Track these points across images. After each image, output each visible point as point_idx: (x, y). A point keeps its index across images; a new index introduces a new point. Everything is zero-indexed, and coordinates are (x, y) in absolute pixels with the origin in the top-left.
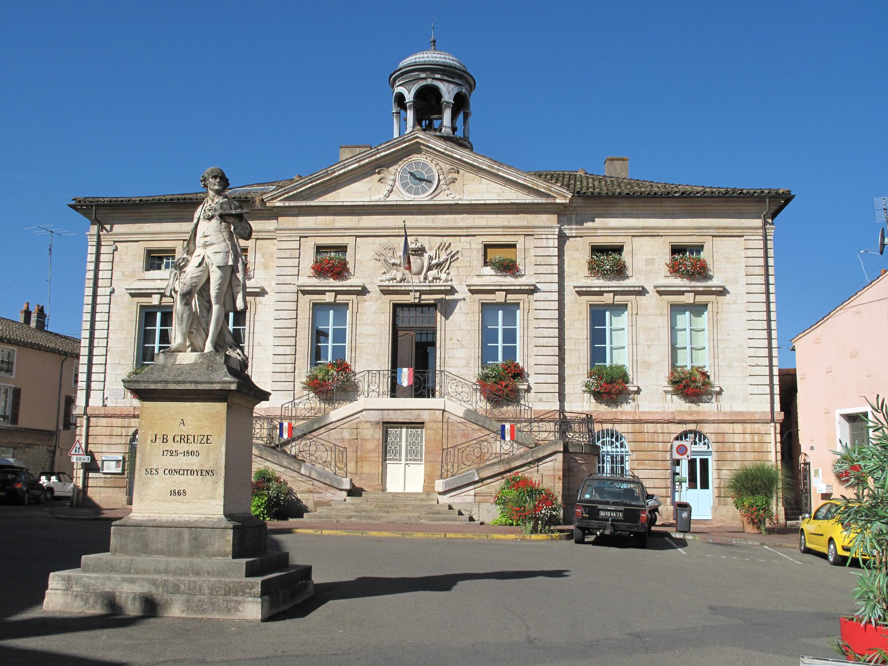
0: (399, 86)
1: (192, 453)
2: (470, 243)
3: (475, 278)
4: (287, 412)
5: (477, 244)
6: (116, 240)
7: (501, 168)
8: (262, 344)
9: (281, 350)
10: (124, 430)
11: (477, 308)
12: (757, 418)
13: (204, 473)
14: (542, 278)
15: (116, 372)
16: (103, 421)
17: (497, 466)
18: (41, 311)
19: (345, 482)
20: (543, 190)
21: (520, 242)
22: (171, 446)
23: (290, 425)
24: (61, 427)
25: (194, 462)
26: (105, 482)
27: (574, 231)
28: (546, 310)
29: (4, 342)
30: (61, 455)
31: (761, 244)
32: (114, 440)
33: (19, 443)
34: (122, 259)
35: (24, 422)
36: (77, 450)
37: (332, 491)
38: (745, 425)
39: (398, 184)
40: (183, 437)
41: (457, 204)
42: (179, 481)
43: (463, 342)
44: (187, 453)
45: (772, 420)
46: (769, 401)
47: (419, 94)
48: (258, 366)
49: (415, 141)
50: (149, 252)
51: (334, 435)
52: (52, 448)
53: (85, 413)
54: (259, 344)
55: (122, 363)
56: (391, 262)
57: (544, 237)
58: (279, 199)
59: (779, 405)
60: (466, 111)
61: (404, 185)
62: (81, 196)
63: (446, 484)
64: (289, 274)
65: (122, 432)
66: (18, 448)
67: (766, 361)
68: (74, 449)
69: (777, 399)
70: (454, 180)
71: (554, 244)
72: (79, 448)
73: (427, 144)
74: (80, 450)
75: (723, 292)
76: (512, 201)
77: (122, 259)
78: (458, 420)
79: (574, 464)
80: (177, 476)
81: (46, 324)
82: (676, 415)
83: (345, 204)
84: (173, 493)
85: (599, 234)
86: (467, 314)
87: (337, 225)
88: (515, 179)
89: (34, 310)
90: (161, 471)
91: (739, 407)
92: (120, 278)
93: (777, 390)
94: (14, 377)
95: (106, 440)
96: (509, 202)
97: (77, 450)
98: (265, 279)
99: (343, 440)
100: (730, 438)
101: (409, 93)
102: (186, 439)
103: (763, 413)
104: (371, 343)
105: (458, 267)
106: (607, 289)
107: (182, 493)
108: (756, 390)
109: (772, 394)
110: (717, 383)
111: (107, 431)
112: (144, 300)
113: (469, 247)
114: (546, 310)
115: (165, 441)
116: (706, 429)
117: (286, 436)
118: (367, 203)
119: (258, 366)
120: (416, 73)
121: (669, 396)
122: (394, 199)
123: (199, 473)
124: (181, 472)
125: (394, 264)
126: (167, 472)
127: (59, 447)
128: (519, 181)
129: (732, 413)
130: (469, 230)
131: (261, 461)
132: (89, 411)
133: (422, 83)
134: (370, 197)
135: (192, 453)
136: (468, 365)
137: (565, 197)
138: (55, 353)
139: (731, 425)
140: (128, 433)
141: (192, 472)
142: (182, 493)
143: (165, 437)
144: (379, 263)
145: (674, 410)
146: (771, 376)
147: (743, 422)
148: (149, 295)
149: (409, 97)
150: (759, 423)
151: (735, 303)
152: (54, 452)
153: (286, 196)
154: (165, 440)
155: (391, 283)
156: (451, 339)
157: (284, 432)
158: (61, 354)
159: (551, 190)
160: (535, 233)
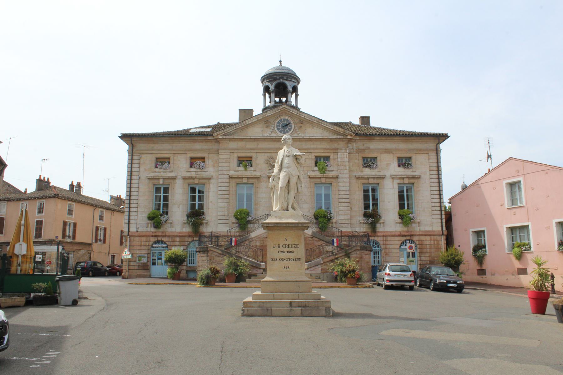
0: (266, 82)
1: (291, 252)
2: (309, 156)
3: (312, 172)
4: (230, 233)
5: (312, 156)
6: (141, 153)
9: (222, 205)
10: (147, 243)
12: (436, 233)
13: (296, 260)
14: (342, 172)
15: (142, 216)
16: (137, 239)
17: (332, 257)
18: (79, 184)
19: (262, 265)
20: (342, 132)
21: (332, 156)
22: (281, 249)
23: (235, 240)
24: (94, 241)
25: (291, 255)
26: (138, 267)
28: (344, 186)
29: (69, 200)
30: (94, 255)
31: (435, 157)
32: (143, 247)
33: (76, 249)
35: (78, 239)
36: (126, 253)
37: (256, 269)
38: (431, 236)
39: (276, 129)
40: (286, 245)
41: (303, 138)
42: (285, 263)
43: (307, 201)
44: (289, 252)
45: (443, 234)
46: (441, 226)
49: (283, 109)
50: (157, 159)
51: (253, 244)
52: (90, 251)
53: (128, 235)
54: (211, 202)
56: (272, 164)
57: (342, 153)
58: (220, 135)
59: (445, 227)
60: (297, 94)
61: (279, 129)
62: (124, 132)
63: (308, 265)
64: (225, 169)
65: (146, 244)
66: (76, 252)
67: (439, 208)
68: (125, 252)
69: (444, 225)
70: (301, 127)
71: (347, 156)
72: (127, 252)
73: (289, 110)
74: (128, 252)
75: (419, 178)
76: (328, 137)
77: (144, 162)
78: (309, 236)
79: (363, 255)
80: (285, 261)
81: (82, 191)
82: (402, 232)
83: (251, 137)
84: (284, 268)
85: (366, 152)
86: (308, 188)
88: (329, 127)
89: (75, 184)
90: (278, 259)
91: (429, 228)
93: (444, 221)
94: (73, 217)
95: (139, 247)
96: (326, 137)
97: (126, 253)
98: (214, 172)
99: (256, 246)
100: (424, 242)
101: (272, 85)
102: (288, 246)
103: (439, 231)
104: (264, 202)
105: (304, 167)
106: (370, 177)
107: (288, 268)
108: (434, 221)
109: (442, 223)
110: (418, 218)
111: (139, 243)
112: (156, 182)
113: (308, 158)
114: (344, 186)
115: (279, 247)
116: (415, 239)
117: (233, 244)
118: (262, 137)
121: (398, 224)
122: (273, 135)
123: (294, 260)
124: (287, 259)
126: (281, 259)
127: (93, 251)
128: (331, 128)
129: (425, 231)
130: (309, 150)
131: (222, 256)
132: (130, 234)
133: (278, 81)
134: (263, 134)
135: (291, 252)
136: (309, 211)
137: (351, 136)
138: (91, 205)
139: (425, 237)
140: (149, 244)
141: (291, 259)
142: (288, 268)
143: (279, 245)
145: (400, 230)
146: (441, 215)
147: (430, 235)
148: (158, 179)
149: (272, 88)
150: (437, 235)
151: (425, 183)
152: (91, 254)
153: (224, 133)
154: (279, 246)
156: (301, 199)
157: (233, 242)
158: (94, 206)
160: (338, 151)
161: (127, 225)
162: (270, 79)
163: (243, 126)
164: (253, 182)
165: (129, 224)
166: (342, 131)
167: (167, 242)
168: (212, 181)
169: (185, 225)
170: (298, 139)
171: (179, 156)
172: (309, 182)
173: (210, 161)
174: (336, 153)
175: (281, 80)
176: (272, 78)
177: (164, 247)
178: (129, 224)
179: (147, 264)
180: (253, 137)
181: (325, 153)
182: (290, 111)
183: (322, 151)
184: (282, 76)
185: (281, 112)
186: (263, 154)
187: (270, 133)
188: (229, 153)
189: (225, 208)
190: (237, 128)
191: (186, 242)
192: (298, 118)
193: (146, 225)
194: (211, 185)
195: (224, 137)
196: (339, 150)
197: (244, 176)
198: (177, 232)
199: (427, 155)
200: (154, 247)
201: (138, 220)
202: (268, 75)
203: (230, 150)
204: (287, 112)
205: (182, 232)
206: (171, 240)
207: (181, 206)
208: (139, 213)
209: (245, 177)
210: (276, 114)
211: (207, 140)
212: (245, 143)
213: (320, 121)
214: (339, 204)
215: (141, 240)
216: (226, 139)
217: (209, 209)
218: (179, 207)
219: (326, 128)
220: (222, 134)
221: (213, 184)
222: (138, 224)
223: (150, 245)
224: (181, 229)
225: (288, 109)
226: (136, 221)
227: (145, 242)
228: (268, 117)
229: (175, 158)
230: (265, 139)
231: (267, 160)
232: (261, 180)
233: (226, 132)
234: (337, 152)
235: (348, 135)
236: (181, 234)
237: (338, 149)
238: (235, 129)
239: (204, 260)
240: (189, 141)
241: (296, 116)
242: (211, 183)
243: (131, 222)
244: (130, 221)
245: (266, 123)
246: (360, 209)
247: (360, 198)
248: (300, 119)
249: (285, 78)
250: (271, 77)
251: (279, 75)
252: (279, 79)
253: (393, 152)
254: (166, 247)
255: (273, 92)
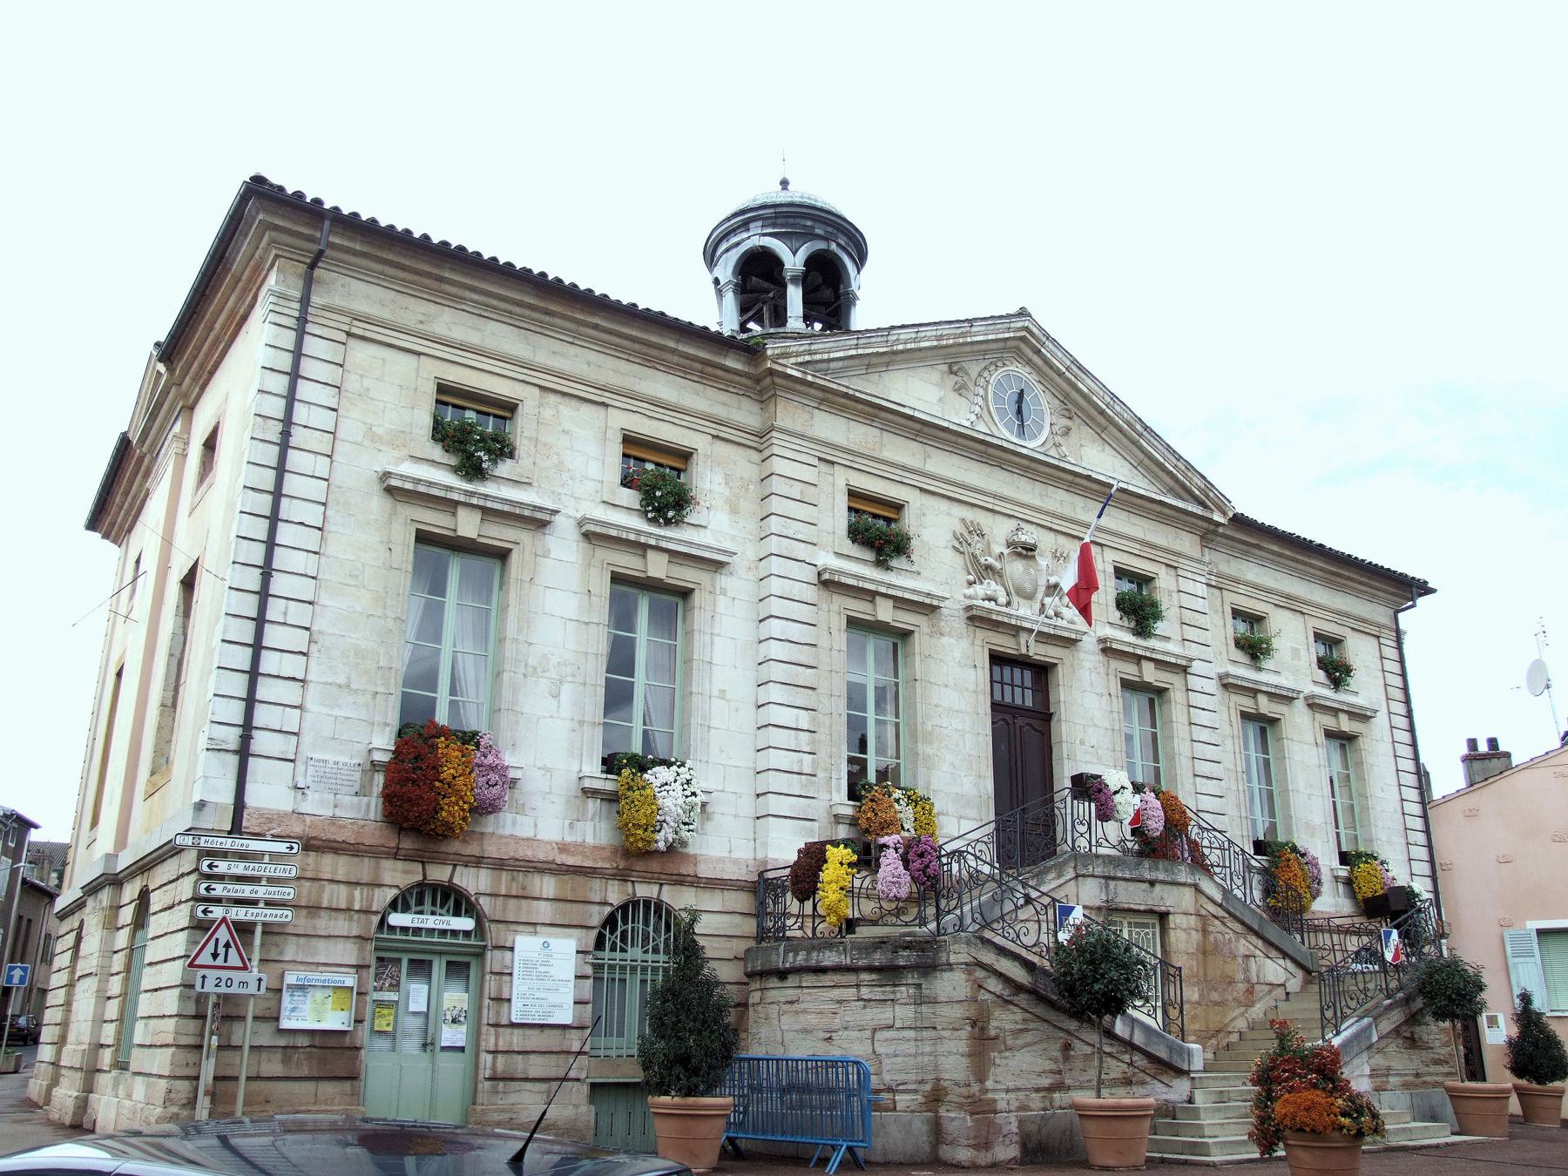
0: (764, 235)
6: (354, 330)
7: (1145, 433)
8: (728, 696)
10: (357, 893)
11: (1115, 687)
15: (336, 712)
20: (1197, 492)
27: (1213, 578)
28: (1203, 709)
34: (368, 389)
36: (221, 950)
47: (813, 262)
48: (722, 751)
55: (354, 686)
56: (982, 560)
58: (793, 360)
70: (1069, 429)
73: (1039, 346)
74: (233, 951)
83: (917, 414)
85: (1241, 591)
87: (888, 455)
92: (359, 439)
97: (221, 950)
101: (794, 254)
114: (1203, 709)
119: (722, 751)
120: (809, 223)
125: (988, 567)
133: (821, 245)
144: (959, 559)
153: (808, 358)
155: (987, 604)
159: (1207, 496)
160: (1181, 566)
161: (233, 760)
162: (782, 226)
163: (884, 350)
164: (911, 628)
165: (244, 752)
166: (1199, 489)
167: (482, 900)
168: (723, 580)
169: (593, 805)
170: (1070, 478)
171: (567, 410)
172: (1102, 670)
173: (719, 478)
174: (1172, 572)
175: (834, 246)
176: (791, 226)
177: (454, 933)
178: (244, 752)
179: (347, 1041)
180: (923, 417)
181: (1141, 560)
182: (1043, 350)
183: (1136, 550)
184: (835, 231)
185: (1009, 344)
186: (944, 505)
187: (973, 417)
188: (815, 462)
189: (801, 733)
190: (860, 351)
191: (596, 908)
192: (1062, 391)
193: (357, 776)
194: (721, 600)
195: (810, 378)
196: (1180, 560)
197: (883, 590)
198: (549, 843)
199: (1374, 641)
200: (392, 929)
201: (306, 739)
202: (778, 210)
203: (823, 449)
204: (1029, 353)
205: (576, 845)
206: (509, 888)
207: (567, 691)
208: (312, 690)
209: (890, 592)
210: (994, 346)
211: (709, 370)
212: (877, 432)
213: (1138, 427)
214: (1198, 779)
215: (317, 870)
216: (813, 391)
217: (713, 731)
218: (556, 696)
219: (1147, 461)
220: (800, 359)
221: (734, 599)
222: (300, 767)
223: (376, 913)
224: (567, 822)
225: (1038, 340)
226: (294, 739)
227: (343, 889)
228: (968, 349)
229: (548, 413)
230: (960, 440)
231: (961, 534)
232: (942, 624)
233: (818, 357)
234: (1176, 568)
235: (1212, 507)
236: (573, 854)
237: (1179, 554)
238: (853, 352)
239: (892, 1027)
240: (625, 343)
241: (1058, 379)
242: (724, 592)
243: (262, 742)
244: (255, 733)
245: (956, 374)
246: (1244, 815)
247: (1239, 769)
248: (1067, 396)
249: (842, 243)
250: (791, 221)
251: (826, 222)
252: (826, 239)
253: (1304, 611)
254: (467, 934)
255: (794, 280)
